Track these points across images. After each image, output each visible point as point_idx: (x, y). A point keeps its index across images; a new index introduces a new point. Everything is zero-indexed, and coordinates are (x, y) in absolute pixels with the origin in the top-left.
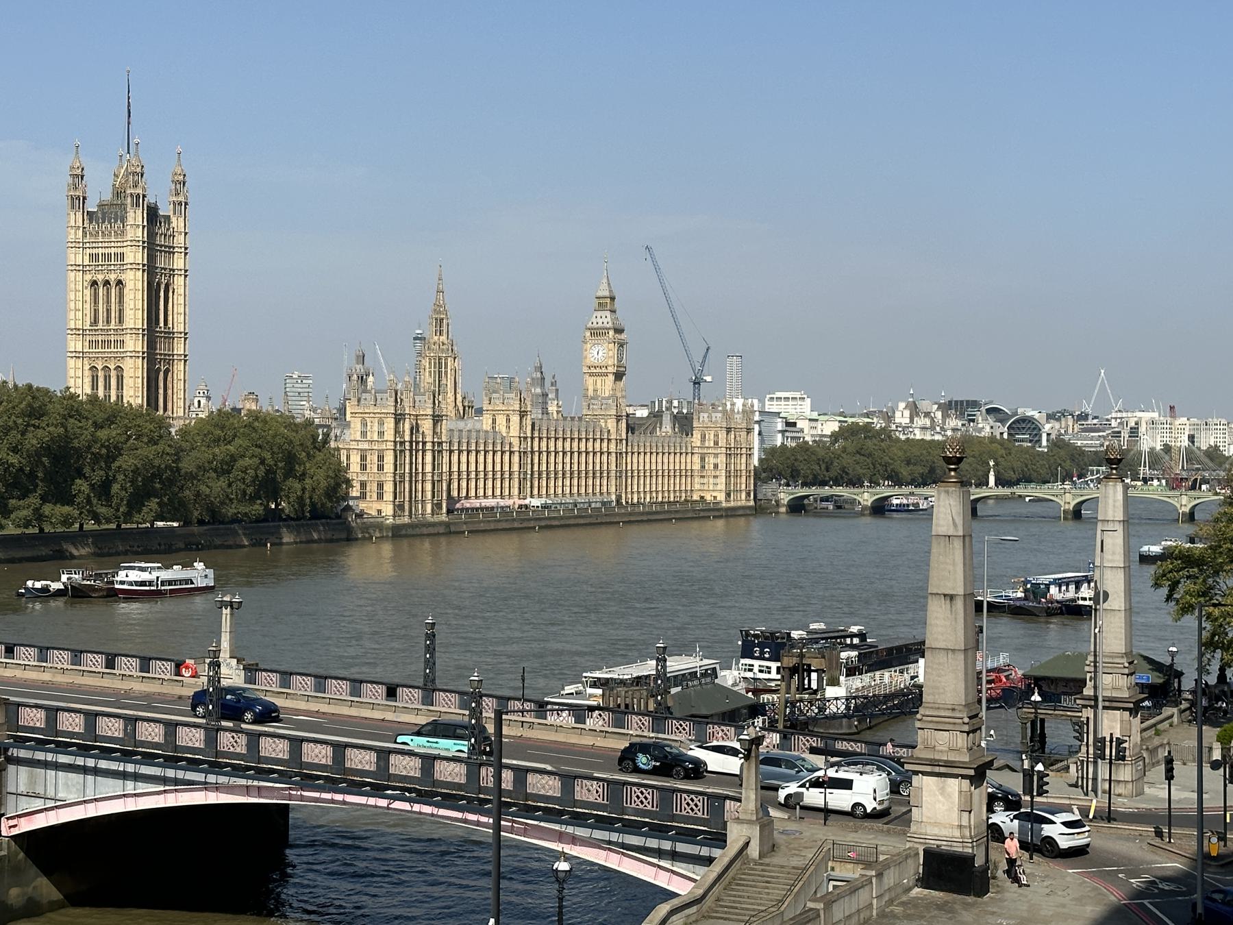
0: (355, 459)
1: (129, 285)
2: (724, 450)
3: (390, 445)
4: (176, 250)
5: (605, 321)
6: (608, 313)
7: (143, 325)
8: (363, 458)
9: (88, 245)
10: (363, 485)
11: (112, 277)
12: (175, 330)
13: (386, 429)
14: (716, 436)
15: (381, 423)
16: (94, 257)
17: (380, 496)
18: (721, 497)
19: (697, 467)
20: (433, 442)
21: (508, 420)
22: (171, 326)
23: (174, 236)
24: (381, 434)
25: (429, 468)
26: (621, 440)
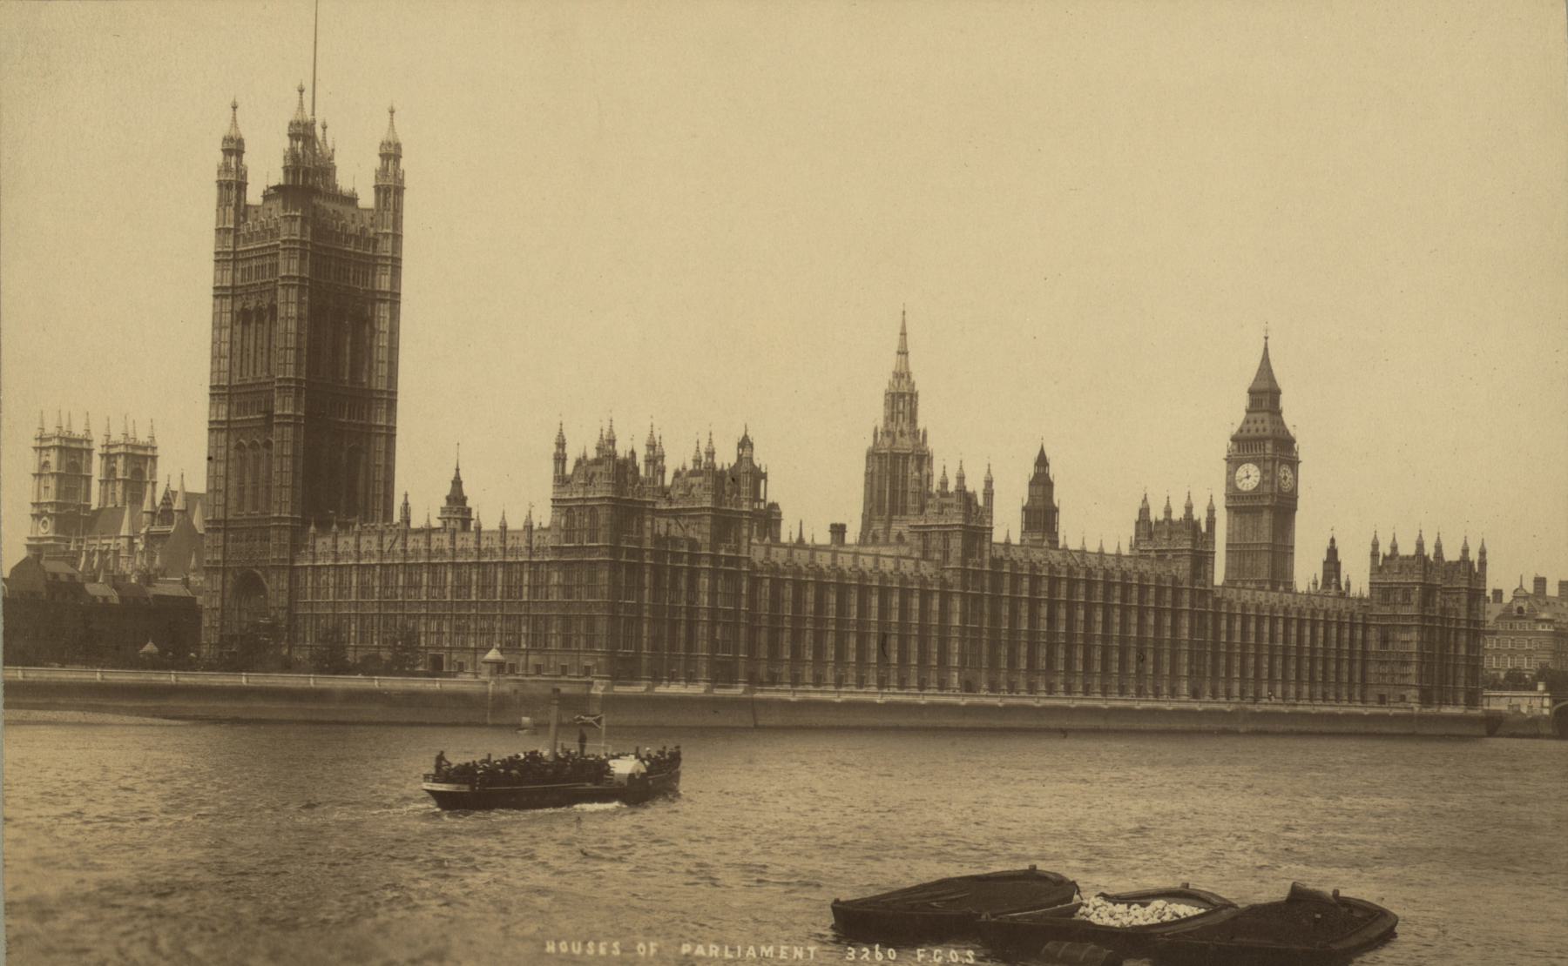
6: (1266, 416)
7: (297, 372)
9: (240, 256)
20: (715, 558)
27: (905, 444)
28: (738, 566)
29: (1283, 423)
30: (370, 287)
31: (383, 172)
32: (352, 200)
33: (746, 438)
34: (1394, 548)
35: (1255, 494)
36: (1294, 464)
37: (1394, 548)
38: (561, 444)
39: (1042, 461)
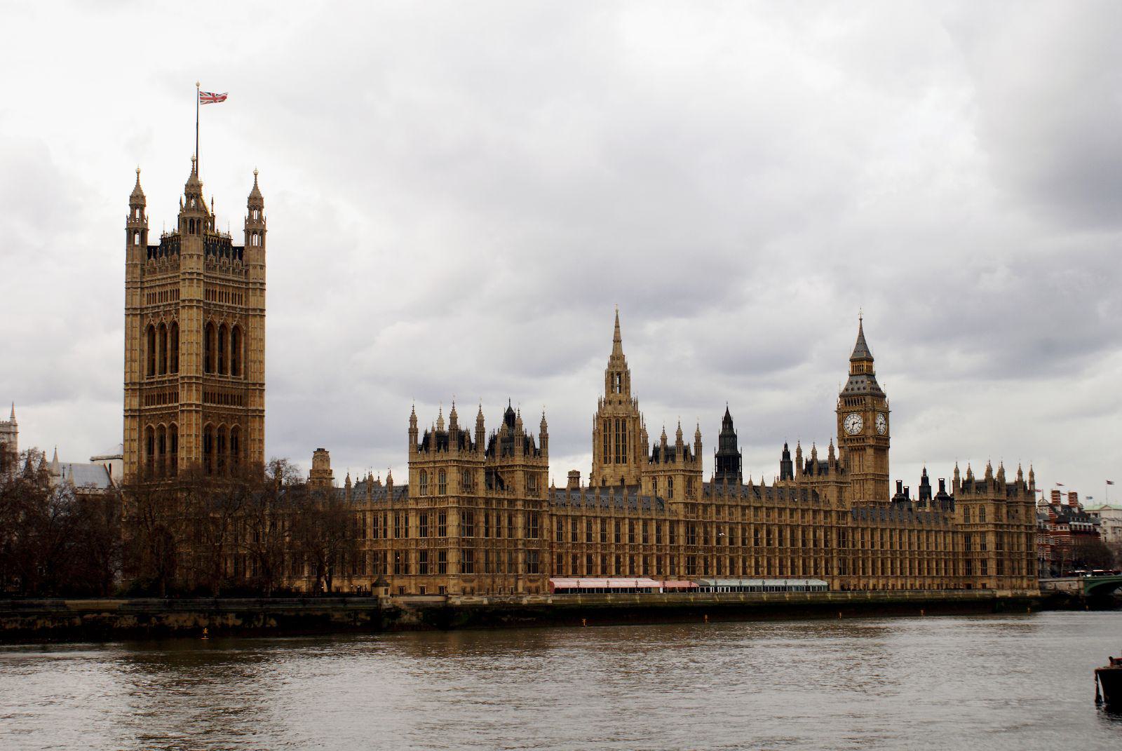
0: (414, 521)
1: (183, 326)
2: (991, 528)
3: (452, 503)
4: (251, 286)
5: (862, 386)
6: (864, 378)
7: (197, 372)
8: (423, 520)
9: (146, 285)
10: (424, 555)
11: (167, 321)
12: (245, 382)
13: (448, 480)
14: (982, 511)
15: (443, 473)
16: (151, 297)
17: (443, 569)
18: (991, 583)
19: (960, 549)
21: (671, 483)
22: (242, 376)
23: (247, 272)
24: (443, 488)
25: (520, 534)
26: (845, 513)
27: (621, 411)
28: (541, 507)
29: (876, 382)
30: (243, 306)
31: (249, 220)
32: (228, 241)
33: (510, 409)
34: (969, 473)
35: (860, 438)
36: (886, 413)
37: (969, 473)
38: (413, 420)
39: (728, 421)
